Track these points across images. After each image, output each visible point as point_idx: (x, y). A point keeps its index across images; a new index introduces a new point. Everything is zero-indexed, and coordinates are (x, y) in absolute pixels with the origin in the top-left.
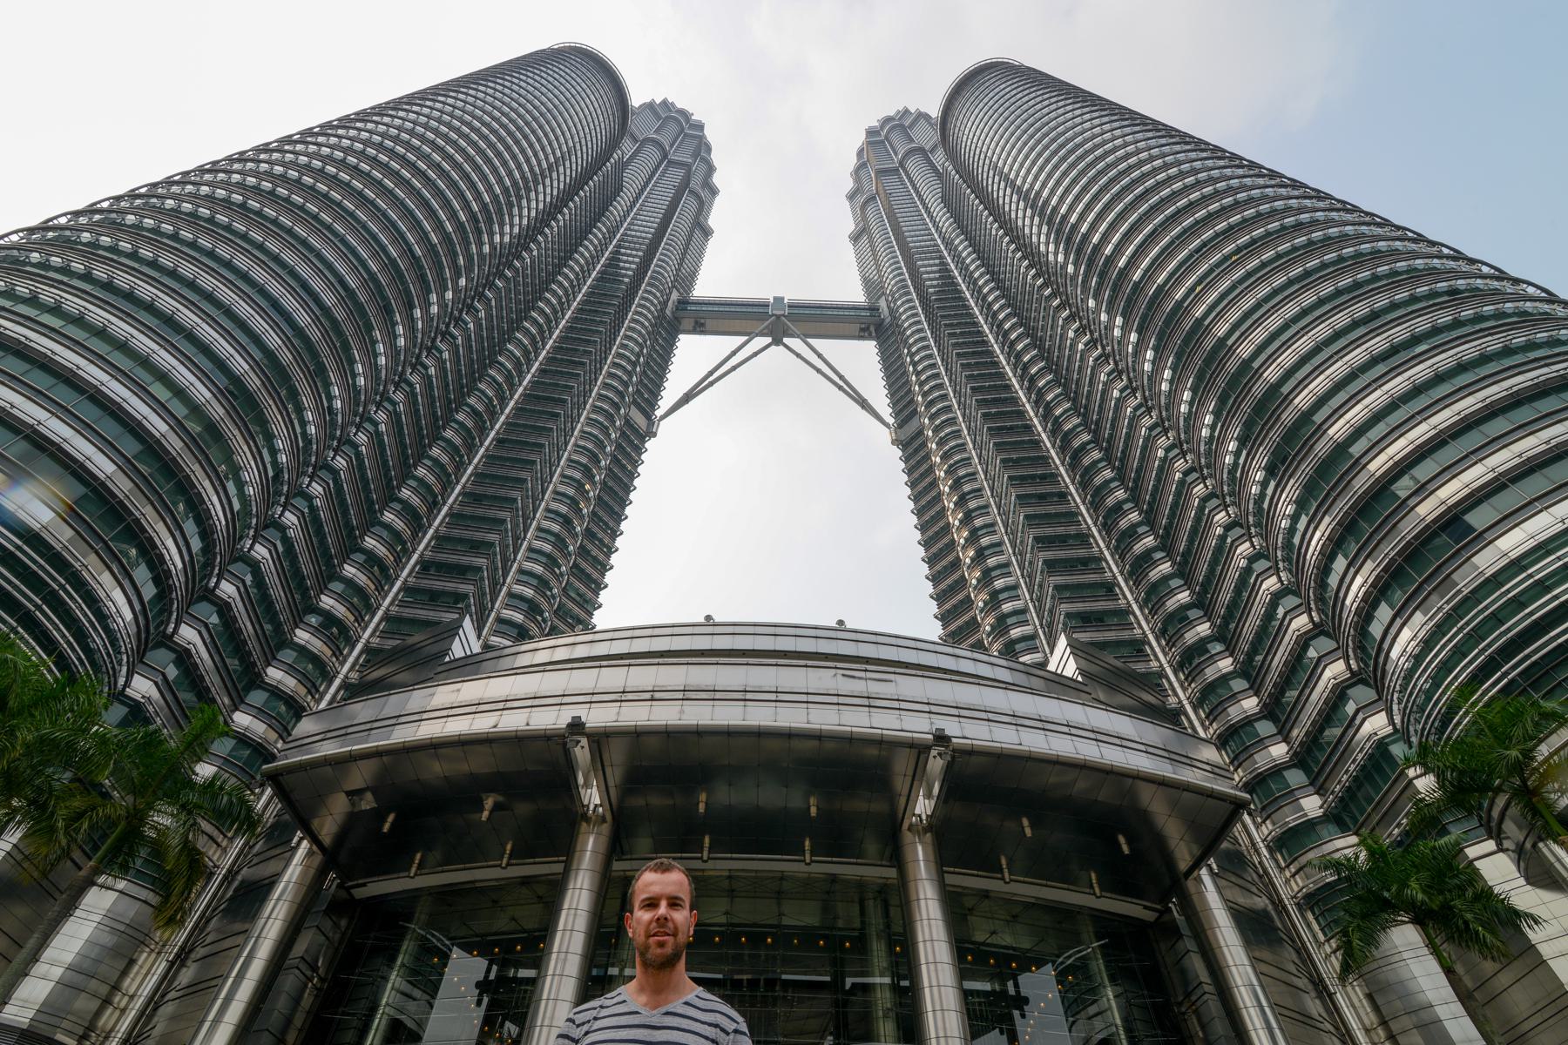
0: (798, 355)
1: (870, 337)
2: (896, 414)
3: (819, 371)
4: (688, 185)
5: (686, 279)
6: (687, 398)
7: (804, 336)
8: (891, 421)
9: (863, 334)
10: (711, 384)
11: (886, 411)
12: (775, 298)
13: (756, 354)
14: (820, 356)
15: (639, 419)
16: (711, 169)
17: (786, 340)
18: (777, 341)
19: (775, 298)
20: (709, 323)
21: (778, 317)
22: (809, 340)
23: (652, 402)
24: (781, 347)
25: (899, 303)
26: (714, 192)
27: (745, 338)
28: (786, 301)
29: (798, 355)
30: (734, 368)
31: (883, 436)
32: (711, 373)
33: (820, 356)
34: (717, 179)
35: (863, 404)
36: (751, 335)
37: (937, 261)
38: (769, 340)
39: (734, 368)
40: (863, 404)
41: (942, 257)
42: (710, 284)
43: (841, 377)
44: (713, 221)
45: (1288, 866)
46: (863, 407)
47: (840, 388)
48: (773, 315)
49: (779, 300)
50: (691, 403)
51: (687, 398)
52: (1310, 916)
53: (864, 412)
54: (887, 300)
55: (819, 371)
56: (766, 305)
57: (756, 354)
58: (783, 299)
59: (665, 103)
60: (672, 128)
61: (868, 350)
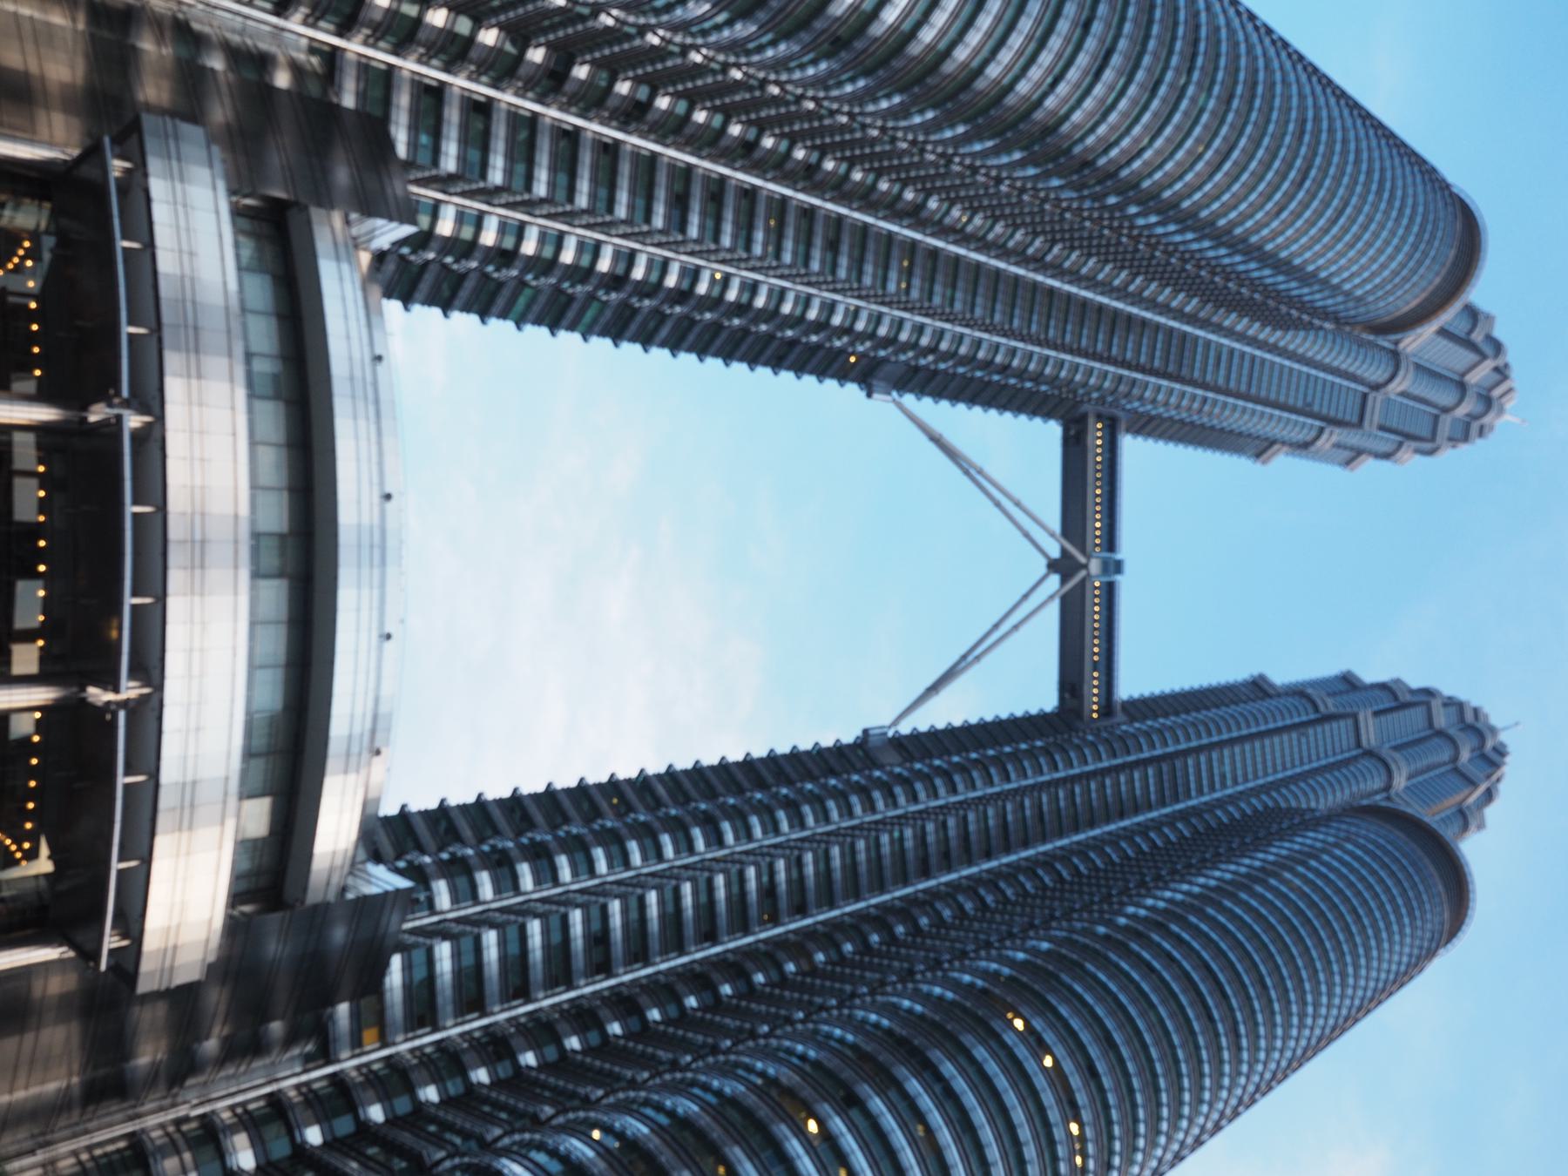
0: (1026, 597)
1: (1062, 698)
6: (937, 440)
9: (1070, 684)
13: (1027, 535)
18: (1053, 566)
21: (1085, 567)
28: (1118, 578)
29: (1026, 597)
32: (980, 472)
35: (934, 689)
37: (1153, 797)
38: (1055, 553)
40: (934, 689)
41: (1163, 804)
43: (978, 658)
44: (1283, 463)
45: (179, 1130)
48: (1089, 557)
50: (932, 447)
51: (937, 440)
52: (122, 1144)
57: (1027, 535)
61: (1043, 696)
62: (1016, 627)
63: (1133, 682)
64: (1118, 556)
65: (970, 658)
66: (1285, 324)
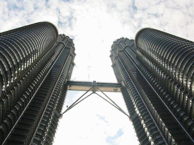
2: (130, 112)
3: (106, 100)
4: (69, 53)
5: (69, 76)
7: (102, 92)
8: (128, 114)
10: (77, 104)
11: (127, 111)
12: (93, 81)
14: (107, 96)
15: (58, 114)
16: (74, 49)
17: (96, 92)
18: (94, 92)
19: (93, 81)
22: (104, 92)
23: (61, 109)
24: (95, 94)
25: (128, 83)
26: (75, 55)
27: (85, 92)
28: (96, 82)
30: (83, 100)
31: (127, 119)
33: (107, 96)
34: (76, 52)
35: (120, 110)
36: (88, 91)
38: (92, 92)
39: (83, 100)
40: (120, 110)
42: (75, 77)
46: (120, 110)
47: (113, 105)
49: (94, 82)
53: (120, 112)
54: (124, 82)
55: (106, 100)
56: (91, 83)
58: (95, 81)
59: (63, 35)
60: (66, 40)
63: (115, 81)
64: (93, 82)
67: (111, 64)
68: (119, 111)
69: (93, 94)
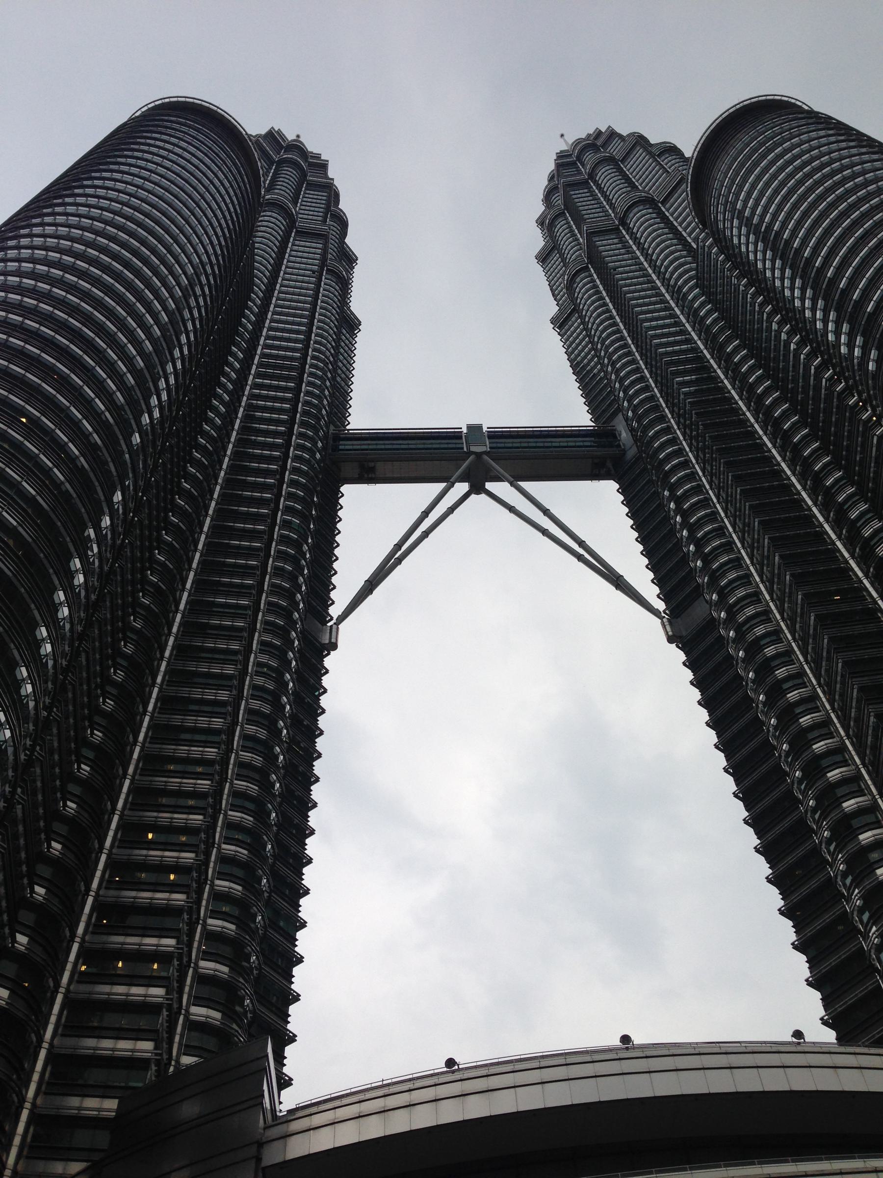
0: (512, 509)
2: (665, 596)
3: (545, 532)
8: (660, 605)
11: (651, 592)
12: (469, 427)
18: (477, 488)
19: (469, 427)
20: (381, 468)
21: (479, 455)
28: (485, 429)
29: (512, 509)
43: (581, 543)
47: (580, 558)
48: (470, 453)
49: (474, 429)
55: (545, 532)
58: (480, 427)
62: (546, 512)
64: (465, 430)
65: (581, 551)
66: (248, 285)
67: (553, 309)
68: (612, 588)
69: (473, 496)
